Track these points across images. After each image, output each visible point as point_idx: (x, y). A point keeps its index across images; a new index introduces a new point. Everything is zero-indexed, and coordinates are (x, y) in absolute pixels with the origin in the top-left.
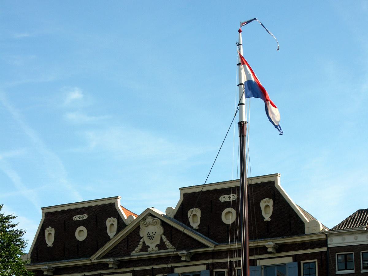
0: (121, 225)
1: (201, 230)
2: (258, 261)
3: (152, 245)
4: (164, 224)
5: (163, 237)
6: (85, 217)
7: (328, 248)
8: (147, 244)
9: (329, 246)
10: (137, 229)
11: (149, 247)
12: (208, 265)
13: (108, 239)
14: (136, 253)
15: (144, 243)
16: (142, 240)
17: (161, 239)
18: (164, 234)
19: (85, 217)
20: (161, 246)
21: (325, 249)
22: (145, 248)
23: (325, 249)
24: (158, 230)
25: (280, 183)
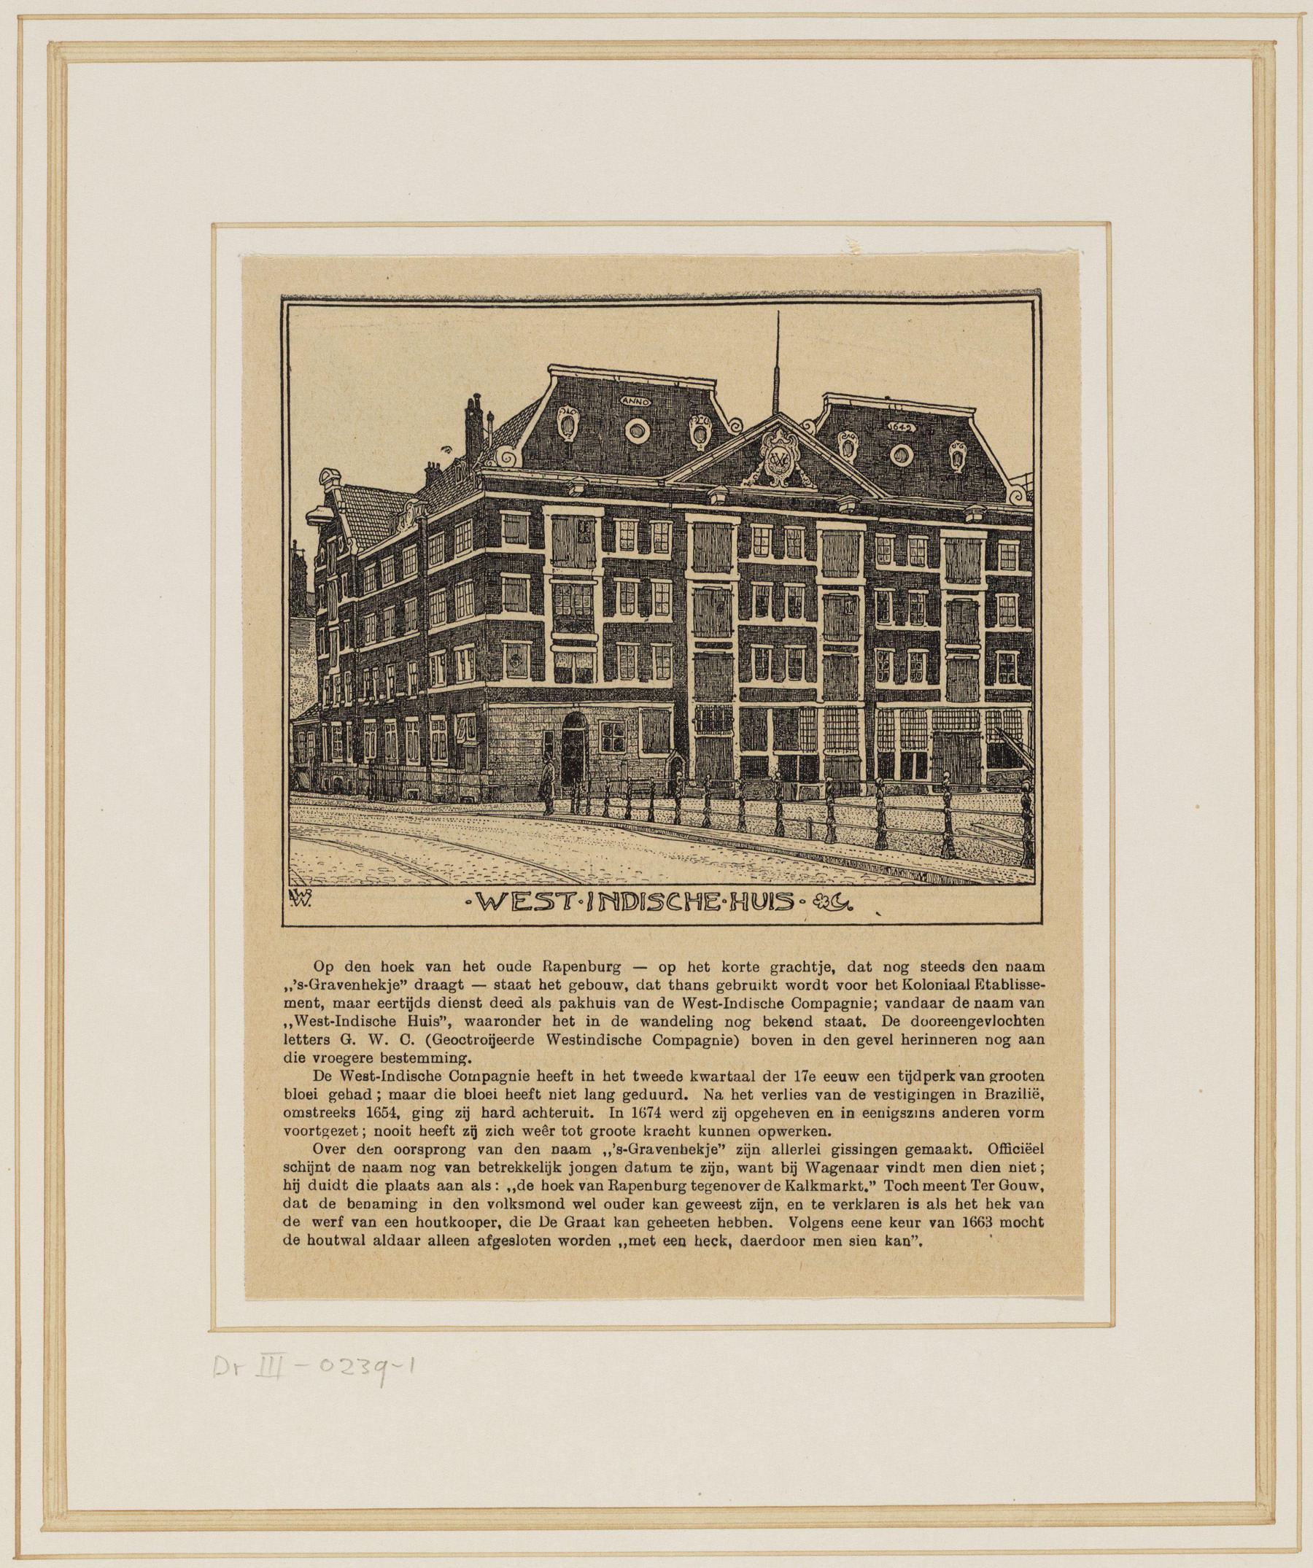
0: (720, 435)
10: (756, 444)
11: (772, 479)
14: (748, 486)
15: (763, 471)
19: (644, 402)
20: (794, 480)
22: (765, 480)
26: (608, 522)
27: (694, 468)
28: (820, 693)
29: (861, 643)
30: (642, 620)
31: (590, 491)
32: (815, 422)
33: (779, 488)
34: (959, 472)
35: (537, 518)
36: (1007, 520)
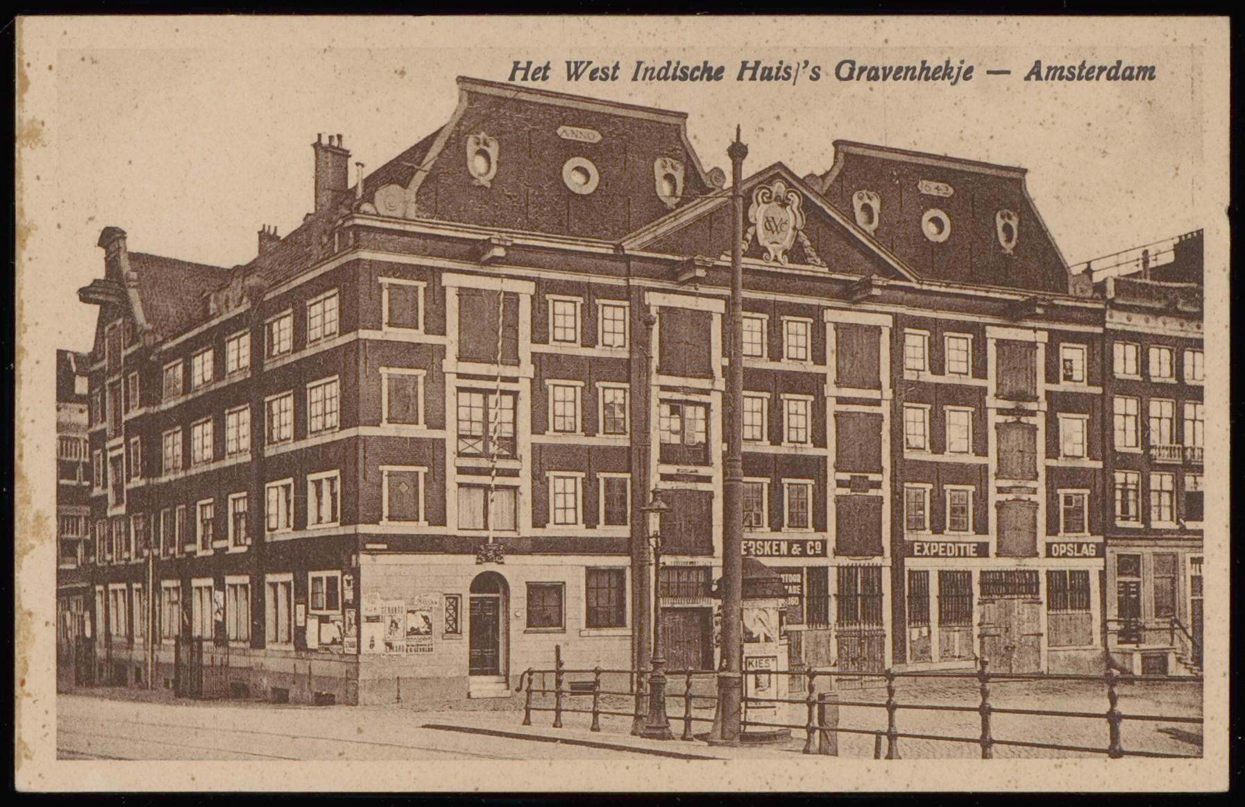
1: (876, 236)
2: (988, 328)
3: (777, 244)
4: (807, 206)
5: (801, 233)
6: (593, 136)
7: (1105, 330)
8: (761, 243)
9: (1108, 326)
11: (765, 250)
12: (896, 316)
13: (660, 210)
15: (755, 236)
16: (751, 230)
17: (798, 235)
18: (806, 230)
19: (593, 136)
20: (796, 254)
21: (1099, 330)
22: (757, 251)
23: (1099, 330)
24: (791, 217)
25: (1038, 190)
26: (539, 305)
27: (661, 231)
28: (831, 545)
29: (886, 479)
30: (772, 450)
31: (519, 256)
32: (824, 177)
33: (777, 260)
34: (1009, 251)
35: (437, 296)
36: (1066, 315)
